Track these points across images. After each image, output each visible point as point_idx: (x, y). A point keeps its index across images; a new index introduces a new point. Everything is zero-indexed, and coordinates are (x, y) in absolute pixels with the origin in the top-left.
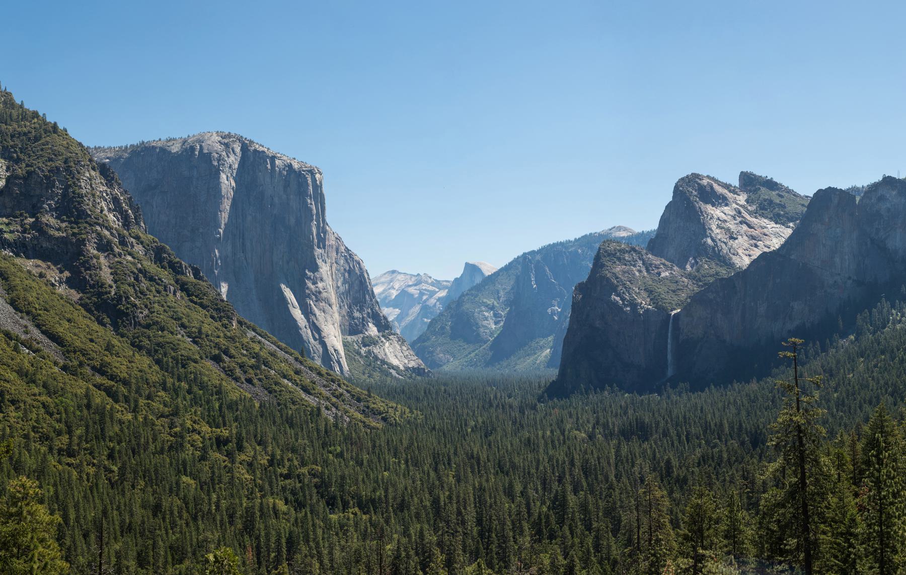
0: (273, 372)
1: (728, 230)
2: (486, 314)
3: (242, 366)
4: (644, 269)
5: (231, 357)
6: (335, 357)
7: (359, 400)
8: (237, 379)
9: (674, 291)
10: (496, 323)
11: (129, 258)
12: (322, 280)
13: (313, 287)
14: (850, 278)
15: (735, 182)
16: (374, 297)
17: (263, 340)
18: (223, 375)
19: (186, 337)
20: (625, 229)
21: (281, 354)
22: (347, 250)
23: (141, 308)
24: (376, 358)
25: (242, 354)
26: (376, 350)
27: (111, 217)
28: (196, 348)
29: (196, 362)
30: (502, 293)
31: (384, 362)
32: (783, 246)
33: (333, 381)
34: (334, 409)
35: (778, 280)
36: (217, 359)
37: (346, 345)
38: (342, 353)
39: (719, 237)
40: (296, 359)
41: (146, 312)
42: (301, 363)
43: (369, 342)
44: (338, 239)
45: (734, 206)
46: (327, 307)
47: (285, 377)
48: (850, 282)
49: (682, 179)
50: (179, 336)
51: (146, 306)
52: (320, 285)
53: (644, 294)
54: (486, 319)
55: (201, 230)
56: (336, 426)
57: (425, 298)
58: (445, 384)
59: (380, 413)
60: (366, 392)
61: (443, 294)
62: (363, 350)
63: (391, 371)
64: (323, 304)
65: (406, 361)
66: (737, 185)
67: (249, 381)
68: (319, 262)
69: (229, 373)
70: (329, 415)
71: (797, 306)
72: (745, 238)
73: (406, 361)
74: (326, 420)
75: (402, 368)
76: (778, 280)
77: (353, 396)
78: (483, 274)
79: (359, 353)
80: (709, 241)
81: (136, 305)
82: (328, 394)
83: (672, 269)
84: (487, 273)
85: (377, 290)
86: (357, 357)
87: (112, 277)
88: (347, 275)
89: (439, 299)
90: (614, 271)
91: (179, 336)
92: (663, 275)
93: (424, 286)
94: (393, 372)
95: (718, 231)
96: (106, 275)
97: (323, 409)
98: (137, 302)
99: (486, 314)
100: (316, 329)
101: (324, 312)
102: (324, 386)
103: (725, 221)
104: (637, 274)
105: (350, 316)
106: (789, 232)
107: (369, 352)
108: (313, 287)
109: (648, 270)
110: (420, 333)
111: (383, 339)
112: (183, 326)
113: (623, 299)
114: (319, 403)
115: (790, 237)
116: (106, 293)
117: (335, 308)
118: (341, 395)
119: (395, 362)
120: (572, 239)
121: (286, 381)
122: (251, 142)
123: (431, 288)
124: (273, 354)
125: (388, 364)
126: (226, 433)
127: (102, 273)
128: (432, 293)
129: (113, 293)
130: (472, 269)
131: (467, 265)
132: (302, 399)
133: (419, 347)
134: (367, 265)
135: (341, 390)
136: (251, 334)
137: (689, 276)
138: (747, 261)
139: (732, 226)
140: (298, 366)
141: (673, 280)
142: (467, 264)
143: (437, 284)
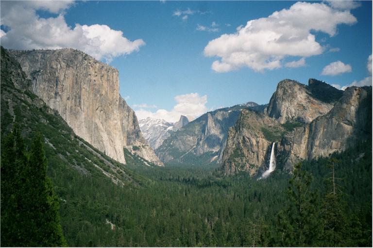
0: (90, 161)
1: (302, 105)
2: (189, 138)
3: (74, 157)
4: (262, 122)
5: (71, 153)
6: (119, 156)
7: (130, 175)
8: (73, 164)
9: (275, 132)
10: (194, 143)
11: (23, 104)
12: (116, 120)
13: (111, 122)
14: (362, 130)
15: (307, 84)
16: (139, 128)
17: (86, 146)
18: (66, 161)
19: (49, 143)
20: (254, 103)
21: (95, 153)
22: (128, 107)
23: (27, 128)
24: (138, 156)
25: (76, 152)
26: (138, 153)
27: (15, 84)
28: (55, 149)
29: (54, 155)
30: (197, 129)
31: (142, 158)
32: (329, 113)
33: (118, 166)
34: (117, 179)
35: (325, 130)
36: (64, 154)
37: (125, 150)
38: (123, 154)
39: (298, 108)
40: (102, 155)
41: (30, 130)
42: (104, 157)
43: (135, 148)
44: (124, 102)
45: (306, 94)
46: (117, 132)
47: (96, 163)
48: (362, 132)
49: (281, 82)
50: (46, 143)
51: (30, 127)
52: (115, 122)
53: (261, 133)
54: (189, 141)
55: (60, 93)
56: (118, 187)
57: (162, 130)
58: (169, 170)
59: (138, 181)
60: (133, 172)
61: (170, 128)
62: (133, 152)
63: (145, 162)
64: (115, 131)
65: (152, 158)
66: (308, 85)
67: (79, 164)
68: (115, 112)
69: (70, 161)
70: (115, 182)
71: (334, 142)
72: (311, 110)
73: (152, 158)
74: (113, 183)
75: (150, 161)
76: (325, 130)
77: (127, 173)
78: (188, 121)
79: (130, 154)
80: (293, 111)
81: (25, 126)
82: (115, 172)
83: (274, 122)
84: (190, 120)
85: (141, 125)
86: (129, 156)
87: (13, 113)
88: (127, 117)
89: (169, 131)
90: (248, 121)
91: (46, 143)
92: (270, 125)
93: (161, 125)
94: (146, 163)
95: (298, 105)
96: (11, 111)
97: (113, 179)
98: (26, 125)
99: (189, 138)
100: (112, 141)
101: (116, 134)
102: (114, 168)
103: (301, 102)
104: (258, 124)
105: (127, 137)
106: (333, 107)
107: (135, 154)
108: (111, 122)
109: (263, 122)
110: (159, 146)
111: (142, 147)
112: (48, 137)
113: (251, 135)
114: (111, 176)
115: (333, 109)
116: (11, 120)
117: (121, 133)
118: (121, 172)
119: (146, 158)
120: (229, 107)
121: (96, 166)
122: (86, 55)
123: (165, 126)
124: (91, 153)
125: (143, 159)
126: (65, 190)
127: (9, 111)
128: (166, 128)
129: (14, 121)
130: (184, 119)
131: (182, 116)
132: (103, 174)
133: (157, 152)
134: (137, 114)
135: (121, 170)
136: (80, 143)
137: (283, 125)
138: (311, 120)
139: (304, 103)
140: (102, 158)
141: (275, 128)
142: (182, 116)
143: (169, 125)
